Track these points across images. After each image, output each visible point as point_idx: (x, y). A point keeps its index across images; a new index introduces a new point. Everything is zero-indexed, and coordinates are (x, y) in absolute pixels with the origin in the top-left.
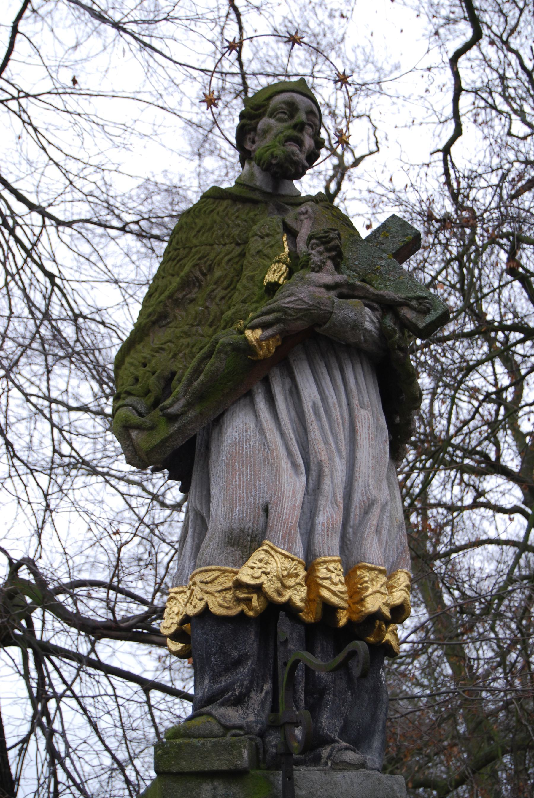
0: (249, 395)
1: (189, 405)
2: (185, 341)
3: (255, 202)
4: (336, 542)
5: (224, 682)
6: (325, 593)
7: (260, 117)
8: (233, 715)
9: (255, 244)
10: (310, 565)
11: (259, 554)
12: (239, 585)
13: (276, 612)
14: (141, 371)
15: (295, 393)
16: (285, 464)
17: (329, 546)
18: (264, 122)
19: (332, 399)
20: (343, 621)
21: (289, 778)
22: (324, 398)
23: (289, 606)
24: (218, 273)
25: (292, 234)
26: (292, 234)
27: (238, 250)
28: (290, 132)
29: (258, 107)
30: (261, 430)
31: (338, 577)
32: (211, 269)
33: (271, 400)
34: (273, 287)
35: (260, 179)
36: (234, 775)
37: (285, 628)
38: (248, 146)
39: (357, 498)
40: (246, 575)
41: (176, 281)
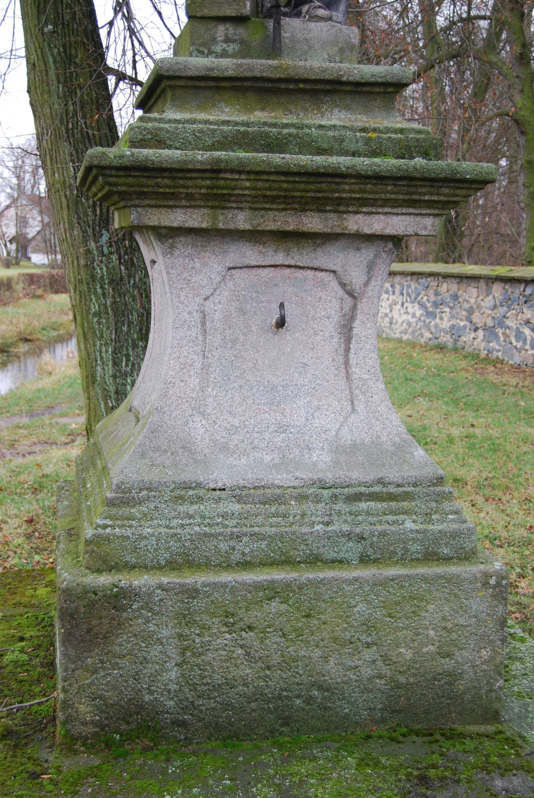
21: (278, 23)
36: (240, 20)
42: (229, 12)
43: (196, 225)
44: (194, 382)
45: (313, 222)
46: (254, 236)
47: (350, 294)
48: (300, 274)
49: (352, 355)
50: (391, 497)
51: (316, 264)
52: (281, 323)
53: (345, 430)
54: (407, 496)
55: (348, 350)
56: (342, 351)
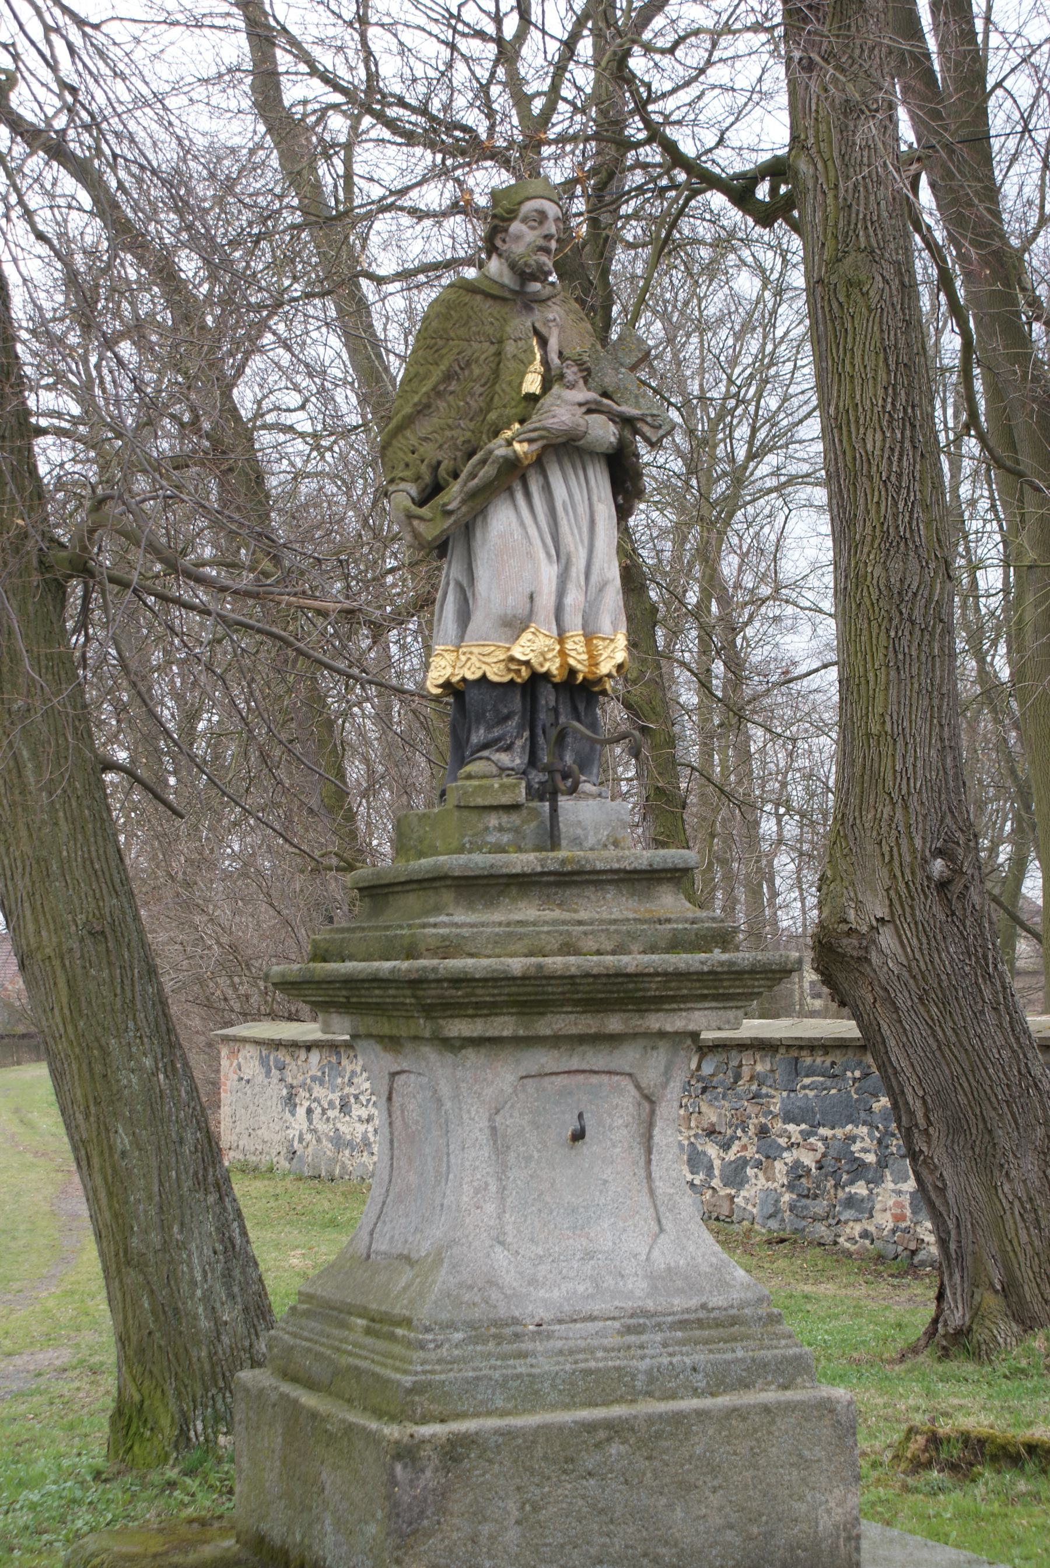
0: (510, 491)
1: (463, 502)
2: (448, 433)
3: (504, 299)
4: (579, 621)
5: (496, 732)
6: (572, 662)
7: (511, 220)
8: (504, 758)
9: (510, 348)
10: (561, 640)
11: (527, 636)
12: (512, 659)
13: (538, 679)
14: (410, 458)
15: (547, 489)
16: (542, 555)
17: (574, 621)
18: (516, 227)
19: (577, 497)
20: (580, 677)
21: (554, 809)
22: (571, 495)
23: (547, 676)
24: (477, 371)
25: (543, 342)
26: (543, 342)
27: (493, 349)
28: (541, 242)
29: (511, 211)
30: (522, 524)
31: (581, 648)
32: (468, 364)
33: (528, 495)
34: (532, 399)
35: (507, 278)
36: (515, 807)
37: (547, 697)
38: (498, 243)
39: (594, 578)
40: (518, 653)
41: (437, 374)
42: (505, 800)
43: (496, 1034)
44: (490, 1208)
45: (614, 1024)
46: (555, 1041)
47: (647, 1098)
48: (594, 1079)
49: (653, 1168)
50: (718, 1324)
51: (613, 1066)
52: (578, 1136)
53: (656, 1253)
54: (734, 1321)
55: (649, 1162)
56: (642, 1163)
